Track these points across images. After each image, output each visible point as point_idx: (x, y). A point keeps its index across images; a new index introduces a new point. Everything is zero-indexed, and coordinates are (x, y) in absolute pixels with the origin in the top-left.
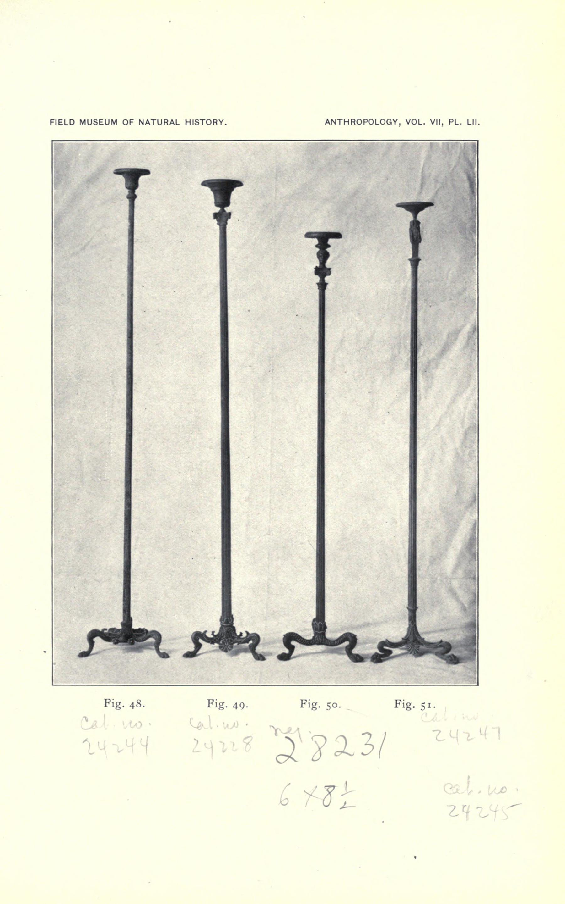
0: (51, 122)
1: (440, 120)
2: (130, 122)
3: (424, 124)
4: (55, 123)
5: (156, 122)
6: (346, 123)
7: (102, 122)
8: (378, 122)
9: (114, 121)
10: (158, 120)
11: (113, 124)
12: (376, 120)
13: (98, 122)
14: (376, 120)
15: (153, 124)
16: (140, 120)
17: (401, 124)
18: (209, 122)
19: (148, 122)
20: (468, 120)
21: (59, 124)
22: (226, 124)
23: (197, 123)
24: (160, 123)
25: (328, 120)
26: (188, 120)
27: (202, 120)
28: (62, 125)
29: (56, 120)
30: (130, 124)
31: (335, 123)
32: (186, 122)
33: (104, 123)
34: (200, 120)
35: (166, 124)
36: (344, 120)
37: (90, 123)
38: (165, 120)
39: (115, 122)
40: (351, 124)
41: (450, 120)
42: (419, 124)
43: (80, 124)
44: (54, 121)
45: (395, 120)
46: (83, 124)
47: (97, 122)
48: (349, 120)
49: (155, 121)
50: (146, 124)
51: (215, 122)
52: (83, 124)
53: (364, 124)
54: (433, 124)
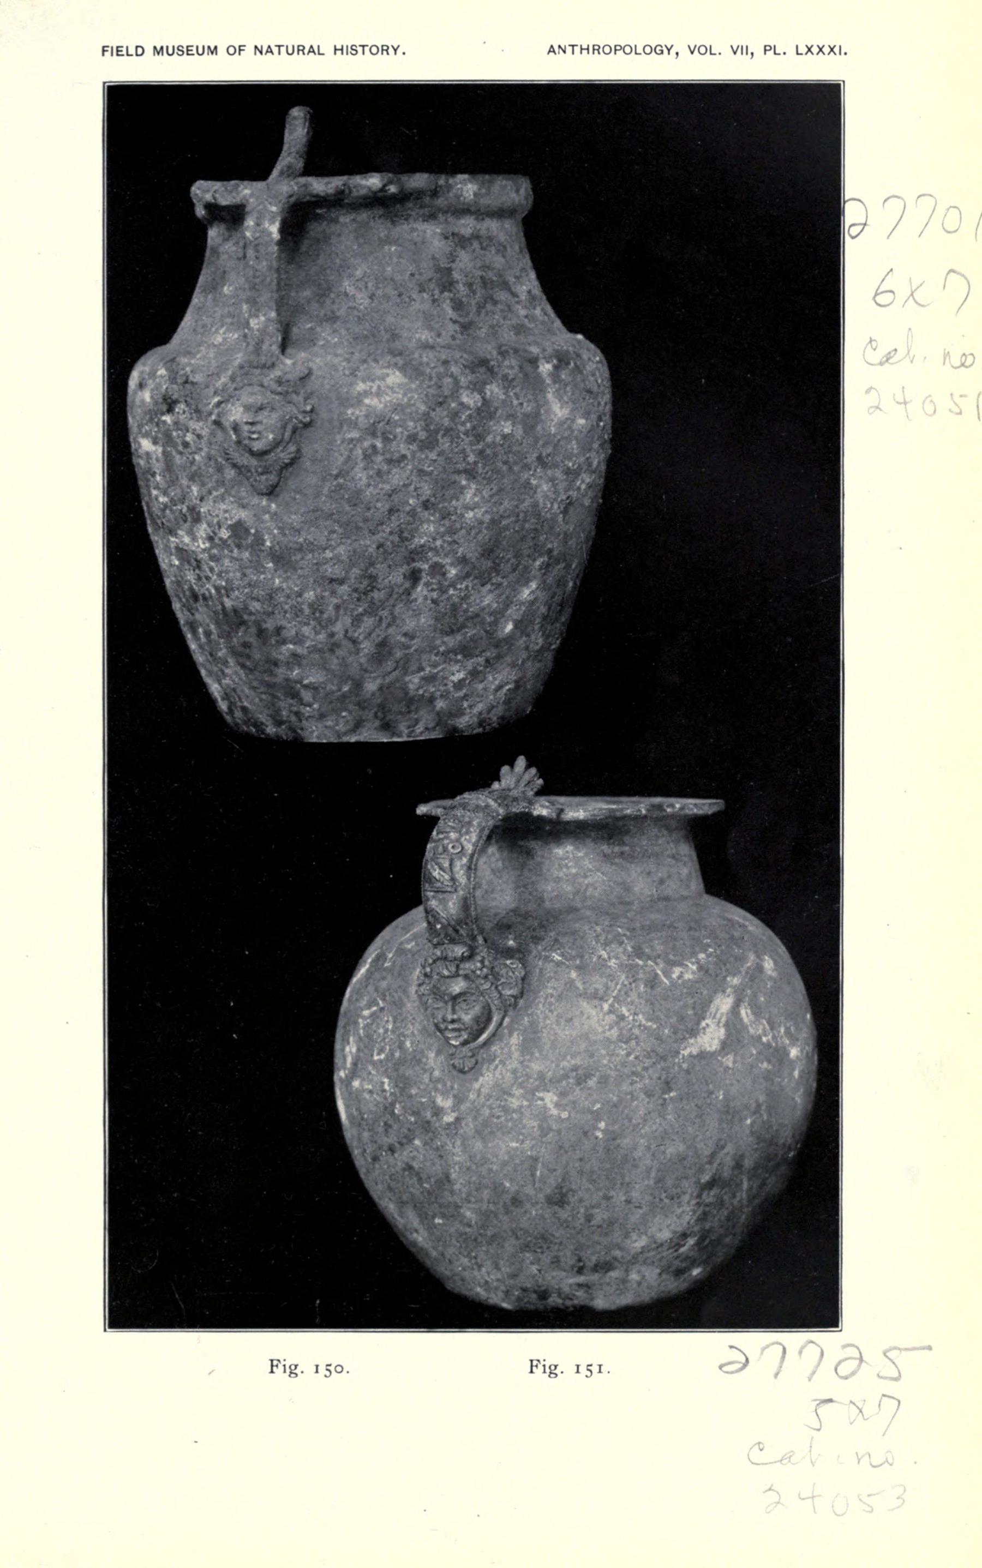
0: (104, 51)
5: (283, 50)
8: (640, 50)
9: (212, 48)
13: (185, 50)
16: (256, 47)
18: (374, 50)
19: (270, 50)
20: (797, 47)
24: (290, 51)
26: (339, 47)
27: (363, 46)
32: (336, 50)
33: (194, 52)
37: (170, 51)
39: (213, 51)
44: (109, 49)
49: (282, 48)
51: (385, 49)
54: (735, 53)
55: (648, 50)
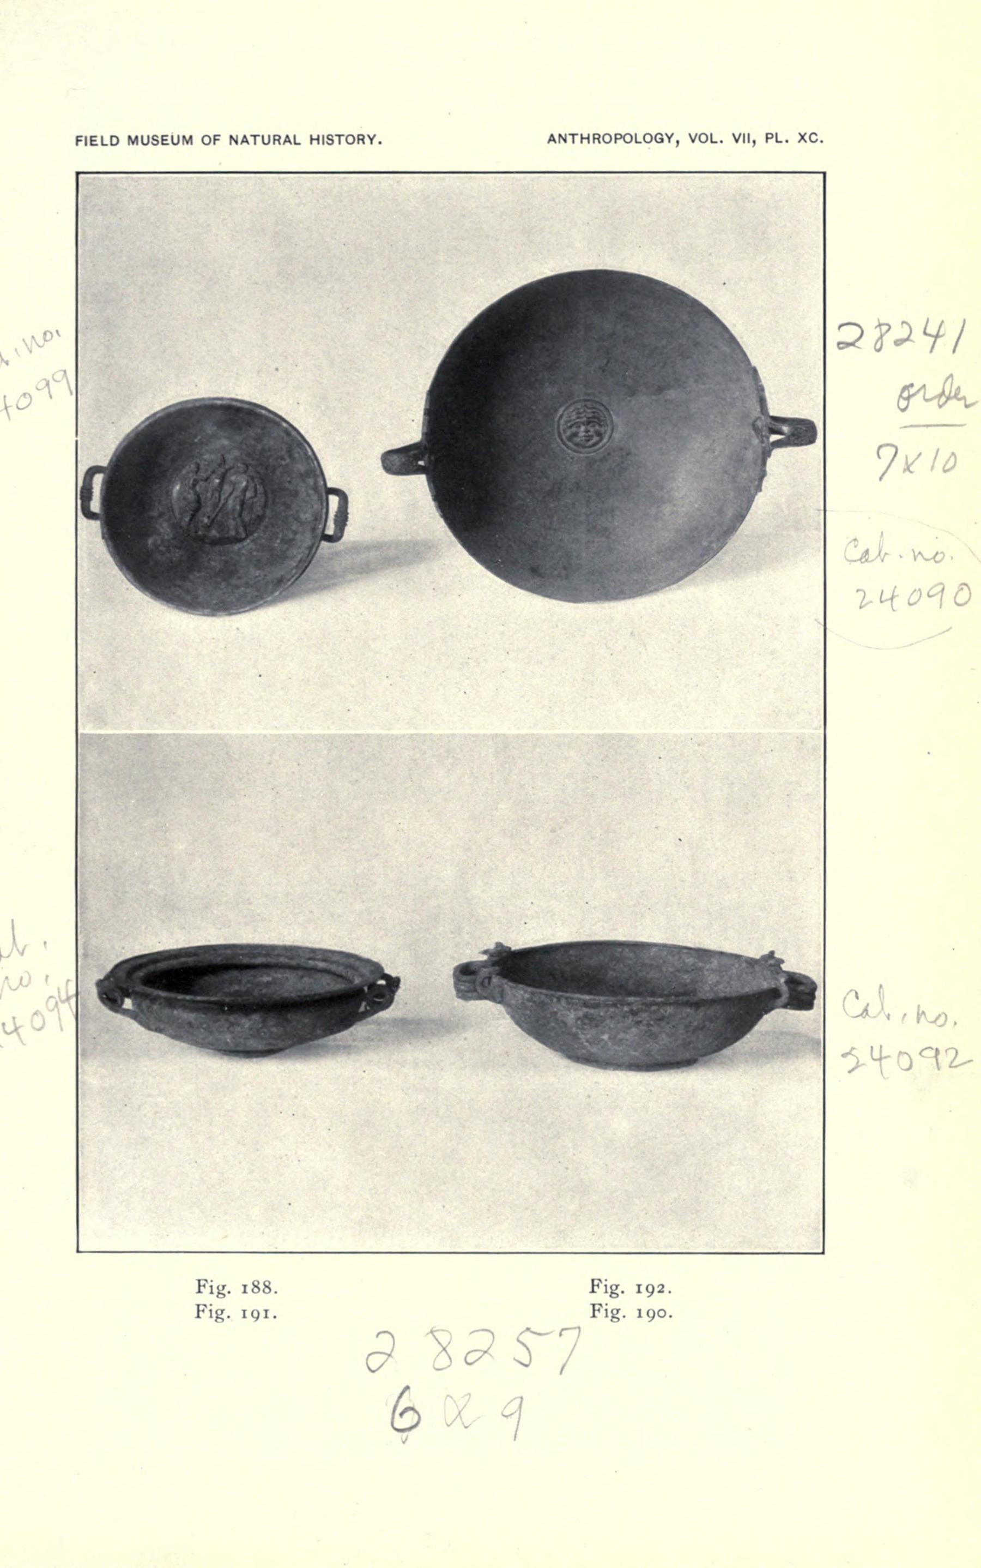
0: (78, 140)
1: (749, 135)
2: (215, 140)
3: (721, 142)
4: (83, 142)
5: (259, 139)
6: (585, 141)
7: (166, 140)
8: (640, 139)
9: (187, 138)
11: (185, 142)
12: (636, 135)
13: (160, 139)
14: (636, 135)
15: (255, 143)
16: (231, 137)
17: (680, 143)
19: (245, 140)
22: (380, 143)
23: (330, 142)
24: (266, 141)
25: (552, 135)
26: (315, 137)
28: (96, 145)
29: (86, 138)
30: (214, 144)
31: (565, 141)
32: (312, 139)
33: (169, 141)
34: (336, 135)
35: (277, 142)
36: (582, 135)
37: (145, 141)
39: (189, 140)
40: (594, 142)
43: (129, 144)
44: (83, 139)
45: (669, 135)
46: (133, 143)
48: (589, 135)
49: (257, 138)
50: (241, 144)
51: (361, 138)
52: (133, 143)
53: (616, 142)
54: (737, 141)
55: (648, 138)
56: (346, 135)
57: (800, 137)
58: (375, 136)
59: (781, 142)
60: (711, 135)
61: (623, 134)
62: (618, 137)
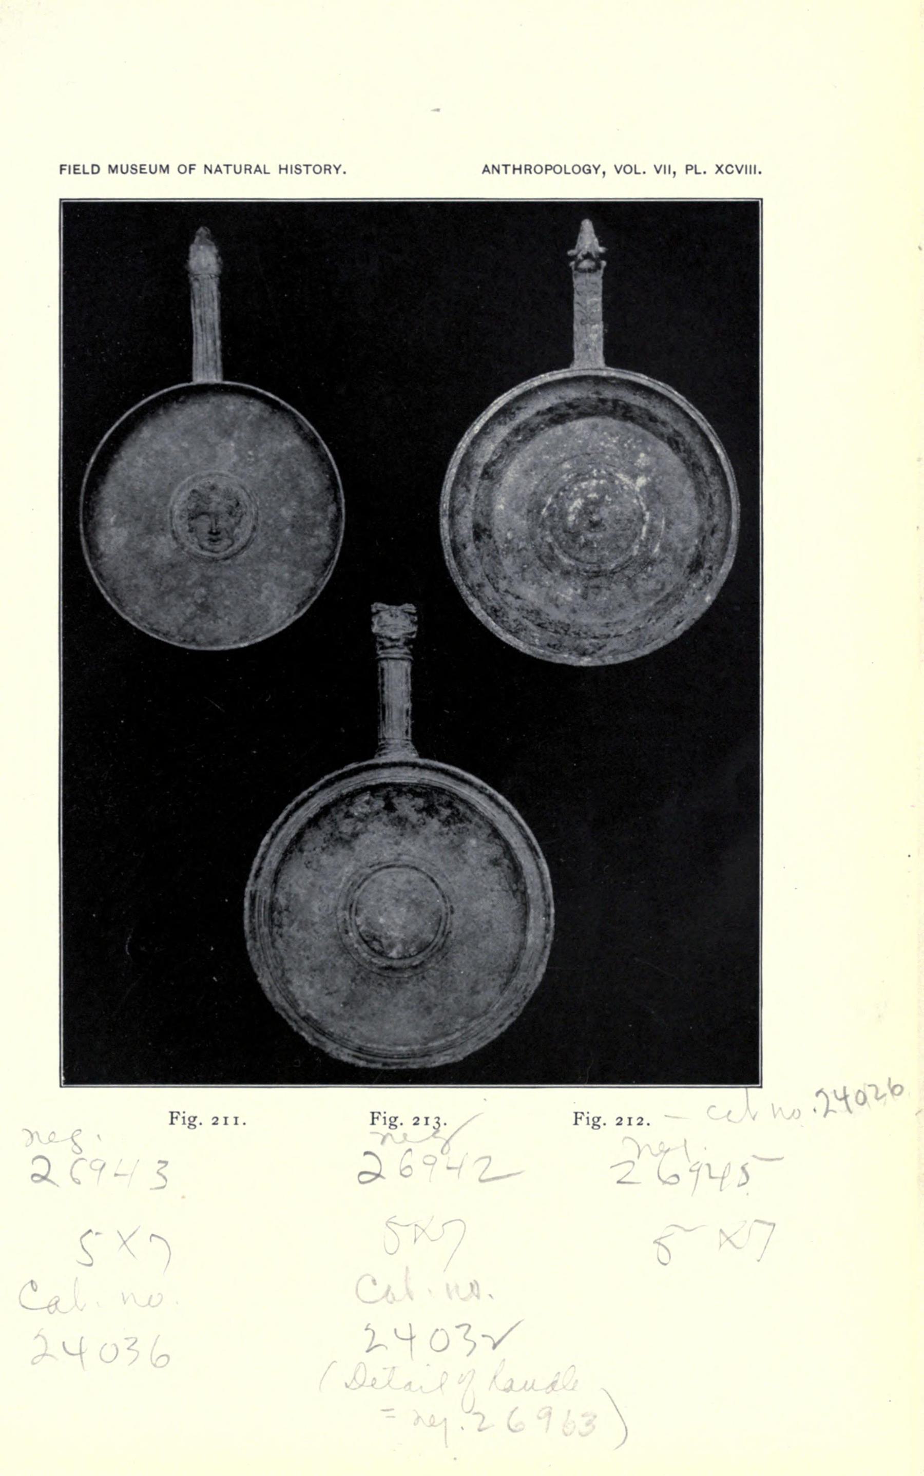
0: (62, 168)
1: (669, 166)
2: (190, 169)
5: (231, 169)
6: (517, 172)
8: (569, 170)
9: (164, 167)
10: (235, 166)
12: (565, 166)
13: (138, 168)
14: (565, 166)
15: (228, 172)
16: (206, 166)
18: (317, 169)
19: (218, 169)
21: (75, 173)
22: (345, 173)
23: (298, 171)
24: (238, 170)
25: (486, 166)
26: (283, 166)
27: (307, 166)
28: (80, 173)
29: (70, 166)
30: (190, 173)
31: (498, 171)
32: (281, 169)
33: (147, 170)
35: (248, 171)
36: (514, 166)
37: (124, 170)
38: (246, 165)
39: (166, 169)
40: (525, 173)
41: (687, 166)
42: (636, 173)
44: (67, 168)
45: (597, 167)
46: (113, 171)
47: (136, 170)
48: (521, 166)
49: (230, 167)
51: (327, 169)
52: (113, 171)
53: (546, 173)
54: (658, 172)
55: (576, 169)
56: (313, 165)
57: (717, 169)
58: (340, 166)
59: (700, 173)
60: (635, 166)
61: (553, 166)
62: (548, 168)
